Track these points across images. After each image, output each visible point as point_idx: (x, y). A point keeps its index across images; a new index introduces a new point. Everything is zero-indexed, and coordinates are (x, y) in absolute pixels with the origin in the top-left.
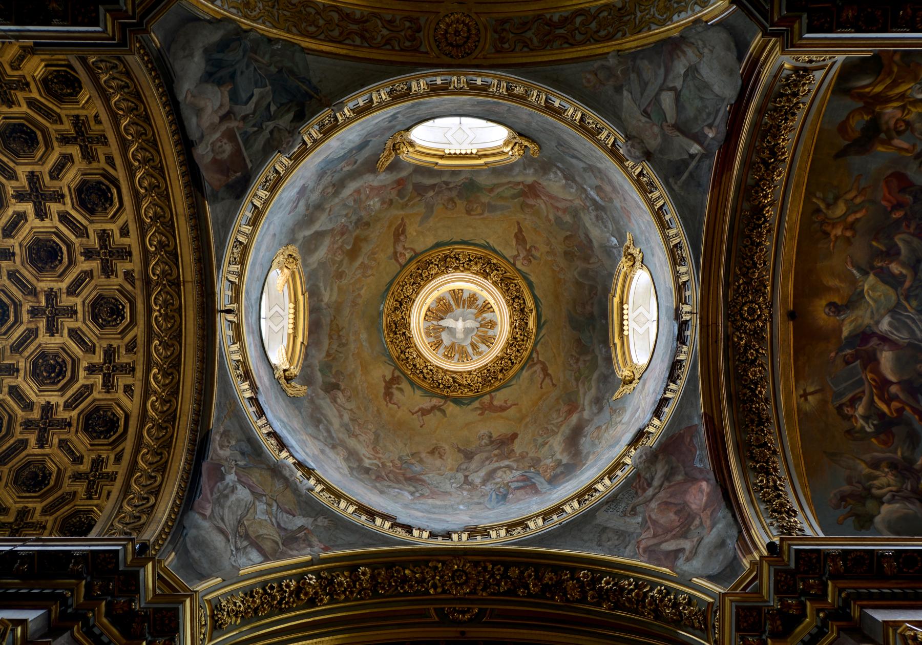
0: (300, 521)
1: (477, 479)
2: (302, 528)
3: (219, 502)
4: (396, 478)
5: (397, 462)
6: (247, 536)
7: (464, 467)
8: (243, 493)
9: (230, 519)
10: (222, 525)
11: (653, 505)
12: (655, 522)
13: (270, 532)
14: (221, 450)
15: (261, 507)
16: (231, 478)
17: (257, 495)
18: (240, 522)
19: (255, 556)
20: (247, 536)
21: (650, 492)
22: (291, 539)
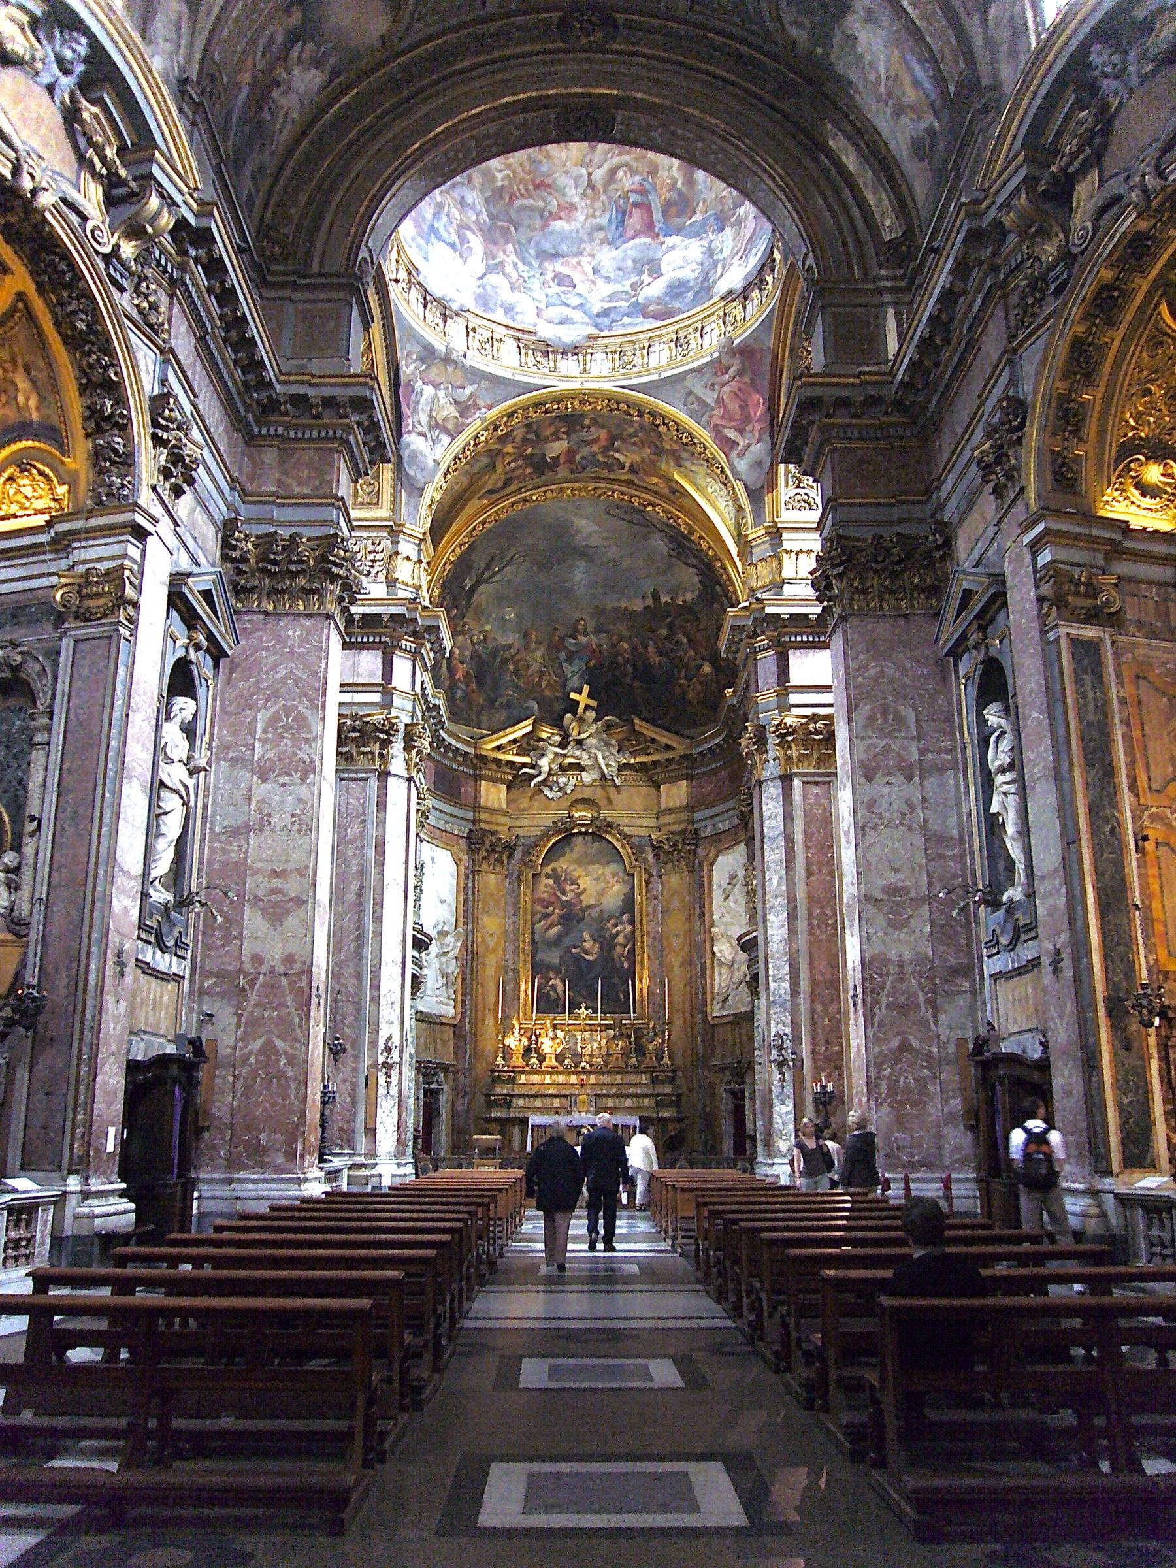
0: (468, 390)
1: (599, 175)
2: (471, 395)
3: (415, 412)
4: (527, 190)
5: (526, 164)
6: (437, 425)
7: (587, 159)
8: (429, 391)
9: (423, 417)
10: (420, 429)
11: (727, 389)
12: (725, 406)
13: (452, 411)
14: (408, 369)
15: (442, 393)
16: (418, 385)
17: (436, 386)
18: (431, 416)
19: (445, 440)
20: (437, 425)
21: (726, 377)
22: (465, 409)
